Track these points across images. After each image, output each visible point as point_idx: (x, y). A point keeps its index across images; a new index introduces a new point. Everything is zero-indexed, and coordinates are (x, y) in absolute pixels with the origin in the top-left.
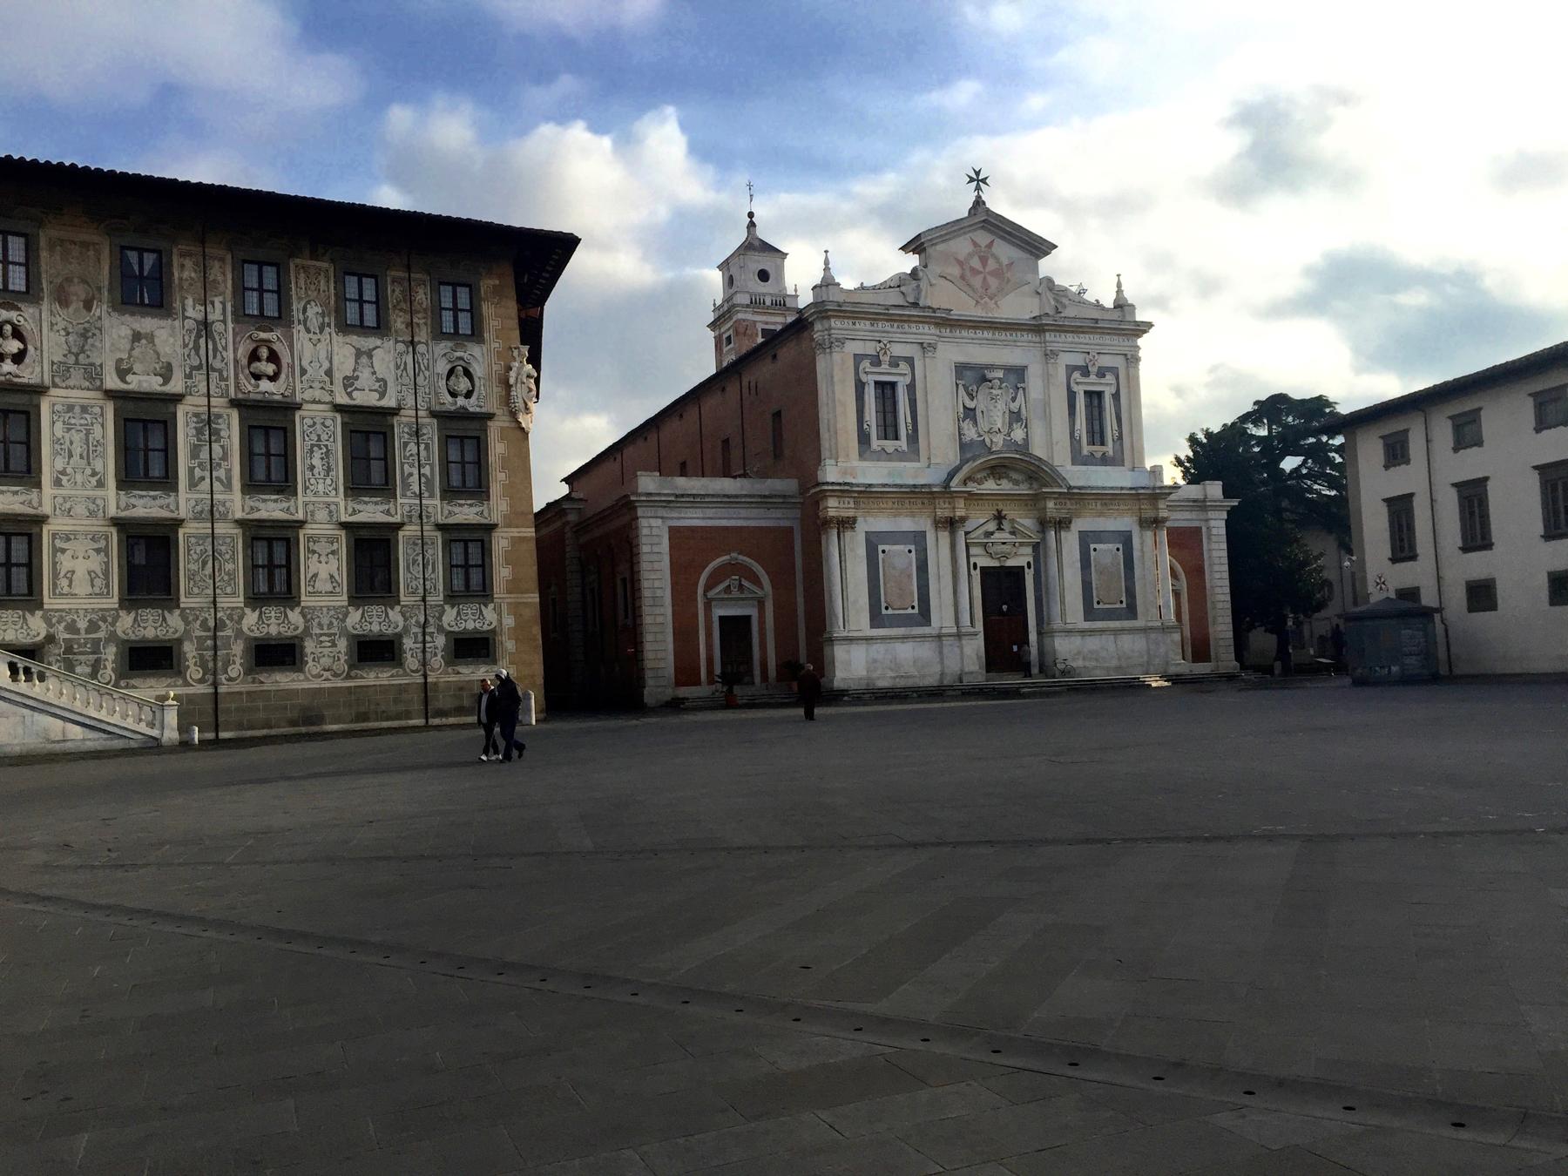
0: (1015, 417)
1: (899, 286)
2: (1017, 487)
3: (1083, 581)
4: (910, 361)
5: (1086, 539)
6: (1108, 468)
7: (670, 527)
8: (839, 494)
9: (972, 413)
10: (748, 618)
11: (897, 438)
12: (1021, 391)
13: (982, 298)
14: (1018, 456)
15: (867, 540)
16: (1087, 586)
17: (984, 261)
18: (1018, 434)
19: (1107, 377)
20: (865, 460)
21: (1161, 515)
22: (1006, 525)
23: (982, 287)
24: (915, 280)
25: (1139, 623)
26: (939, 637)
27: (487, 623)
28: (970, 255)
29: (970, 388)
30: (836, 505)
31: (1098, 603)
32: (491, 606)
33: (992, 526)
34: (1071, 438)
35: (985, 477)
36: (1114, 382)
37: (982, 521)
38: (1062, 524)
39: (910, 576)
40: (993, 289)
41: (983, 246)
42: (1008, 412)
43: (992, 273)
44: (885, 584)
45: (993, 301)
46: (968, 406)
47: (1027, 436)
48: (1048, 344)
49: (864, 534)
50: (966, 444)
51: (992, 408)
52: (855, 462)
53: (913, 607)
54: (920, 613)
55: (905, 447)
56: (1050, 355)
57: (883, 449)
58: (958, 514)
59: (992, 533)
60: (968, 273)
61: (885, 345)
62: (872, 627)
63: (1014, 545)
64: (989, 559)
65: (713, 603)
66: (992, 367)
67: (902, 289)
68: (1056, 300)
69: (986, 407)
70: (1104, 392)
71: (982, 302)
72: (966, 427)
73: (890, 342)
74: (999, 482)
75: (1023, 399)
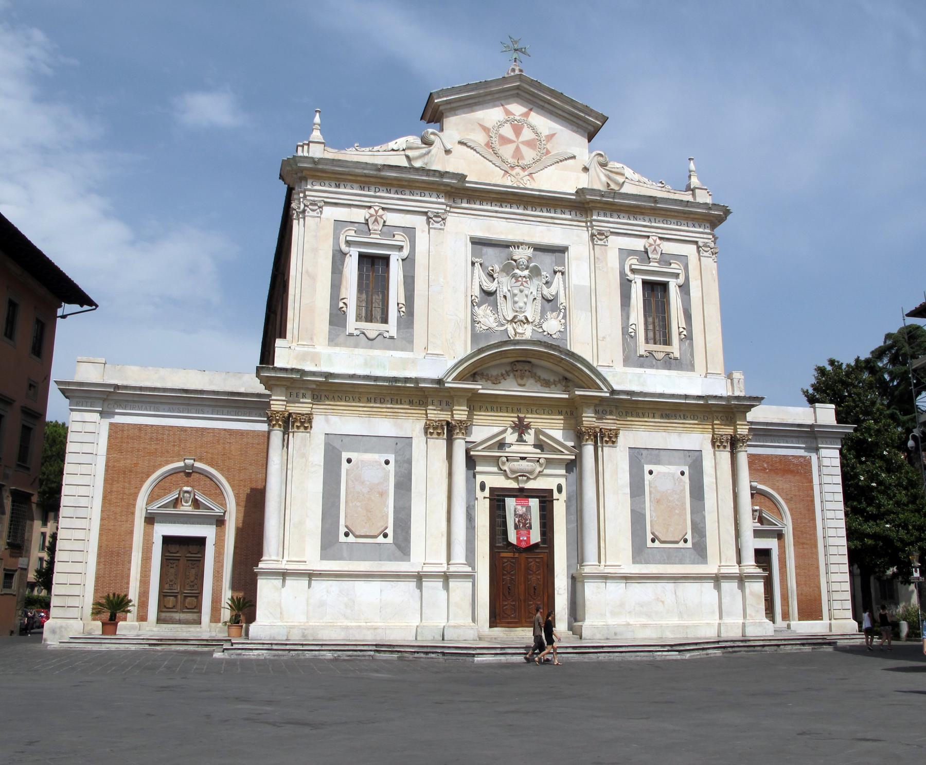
1: (404, 150)
2: (547, 390)
3: (633, 512)
4: (410, 232)
5: (637, 456)
6: (673, 373)
7: (111, 424)
8: (288, 384)
9: (492, 298)
10: (200, 542)
11: (385, 320)
12: (559, 275)
13: (512, 168)
16: (638, 519)
17: (517, 130)
18: (552, 325)
19: (673, 266)
20: (336, 345)
21: (740, 431)
22: (530, 437)
23: (513, 157)
24: (425, 144)
25: (711, 568)
26: (419, 578)
28: (501, 125)
31: (653, 541)
33: (511, 437)
34: (623, 334)
35: (502, 375)
36: (682, 273)
37: (496, 430)
38: (607, 438)
39: (383, 494)
40: (527, 160)
41: (517, 114)
42: (539, 298)
43: (530, 144)
45: (526, 173)
46: (485, 288)
47: (565, 328)
48: (594, 223)
49: (323, 437)
50: (481, 334)
51: (516, 291)
53: (385, 536)
54: (395, 543)
56: (597, 237)
58: (457, 417)
59: (510, 445)
60: (496, 141)
61: (376, 212)
62: (324, 557)
63: (538, 461)
64: (503, 478)
66: (517, 245)
67: (409, 153)
68: (609, 178)
69: (509, 291)
70: (668, 282)
71: (514, 173)
73: (383, 209)
74: (521, 382)
75: (562, 285)
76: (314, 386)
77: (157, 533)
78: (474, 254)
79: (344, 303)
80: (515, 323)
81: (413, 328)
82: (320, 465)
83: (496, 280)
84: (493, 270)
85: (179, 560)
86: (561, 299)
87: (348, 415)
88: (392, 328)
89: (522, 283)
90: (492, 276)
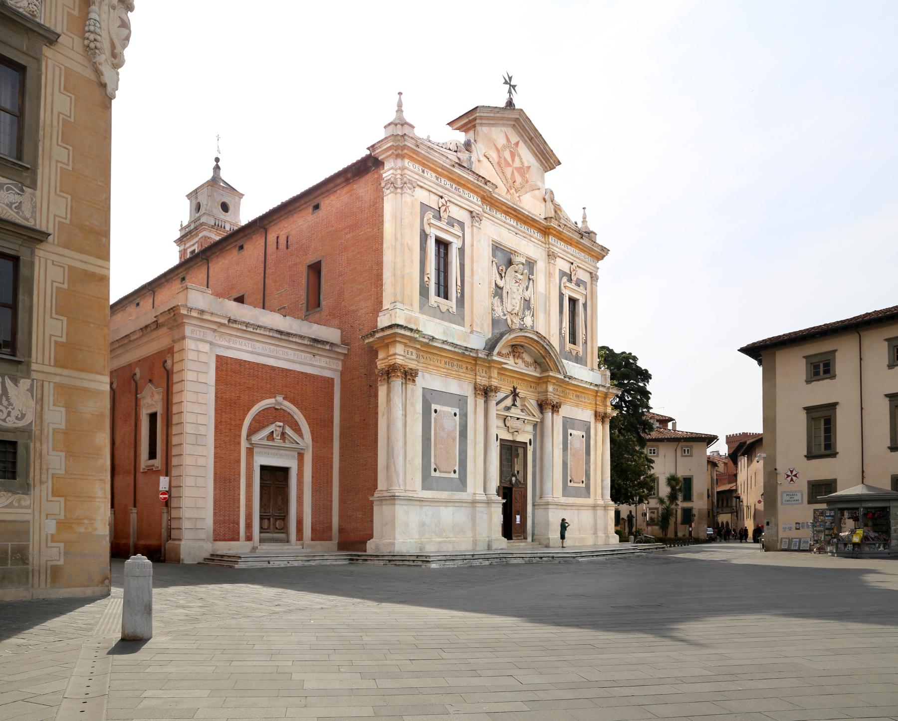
0: (527, 304)
9: (499, 291)
14: (536, 338)
15: (424, 396)
19: (581, 288)
27: (14, 413)
29: (500, 268)
30: (402, 353)
32: (25, 384)
42: (523, 298)
44: (435, 444)
46: (498, 284)
49: (421, 390)
51: (515, 290)
52: (417, 315)
55: (454, 309)
57: (438, 306)
65: (256, 450)
72: (495, 302)
75: (532, 291)
76: (419, 347)
77: (256, 462)
78: (494, 255)
79: (428, 277)
80: (512, 314)
81: (464, 308)
82: (420, 414)
83: (504, 278)
84: (502, 270)
85: (270, 487)
86: (532, 301)
87: (435, 374)
88: (451, 304)
89: (519, 286)
90: (501, 274)
